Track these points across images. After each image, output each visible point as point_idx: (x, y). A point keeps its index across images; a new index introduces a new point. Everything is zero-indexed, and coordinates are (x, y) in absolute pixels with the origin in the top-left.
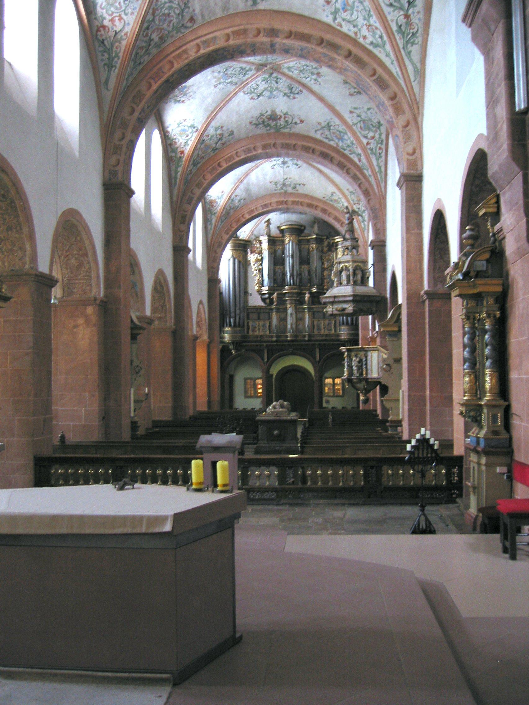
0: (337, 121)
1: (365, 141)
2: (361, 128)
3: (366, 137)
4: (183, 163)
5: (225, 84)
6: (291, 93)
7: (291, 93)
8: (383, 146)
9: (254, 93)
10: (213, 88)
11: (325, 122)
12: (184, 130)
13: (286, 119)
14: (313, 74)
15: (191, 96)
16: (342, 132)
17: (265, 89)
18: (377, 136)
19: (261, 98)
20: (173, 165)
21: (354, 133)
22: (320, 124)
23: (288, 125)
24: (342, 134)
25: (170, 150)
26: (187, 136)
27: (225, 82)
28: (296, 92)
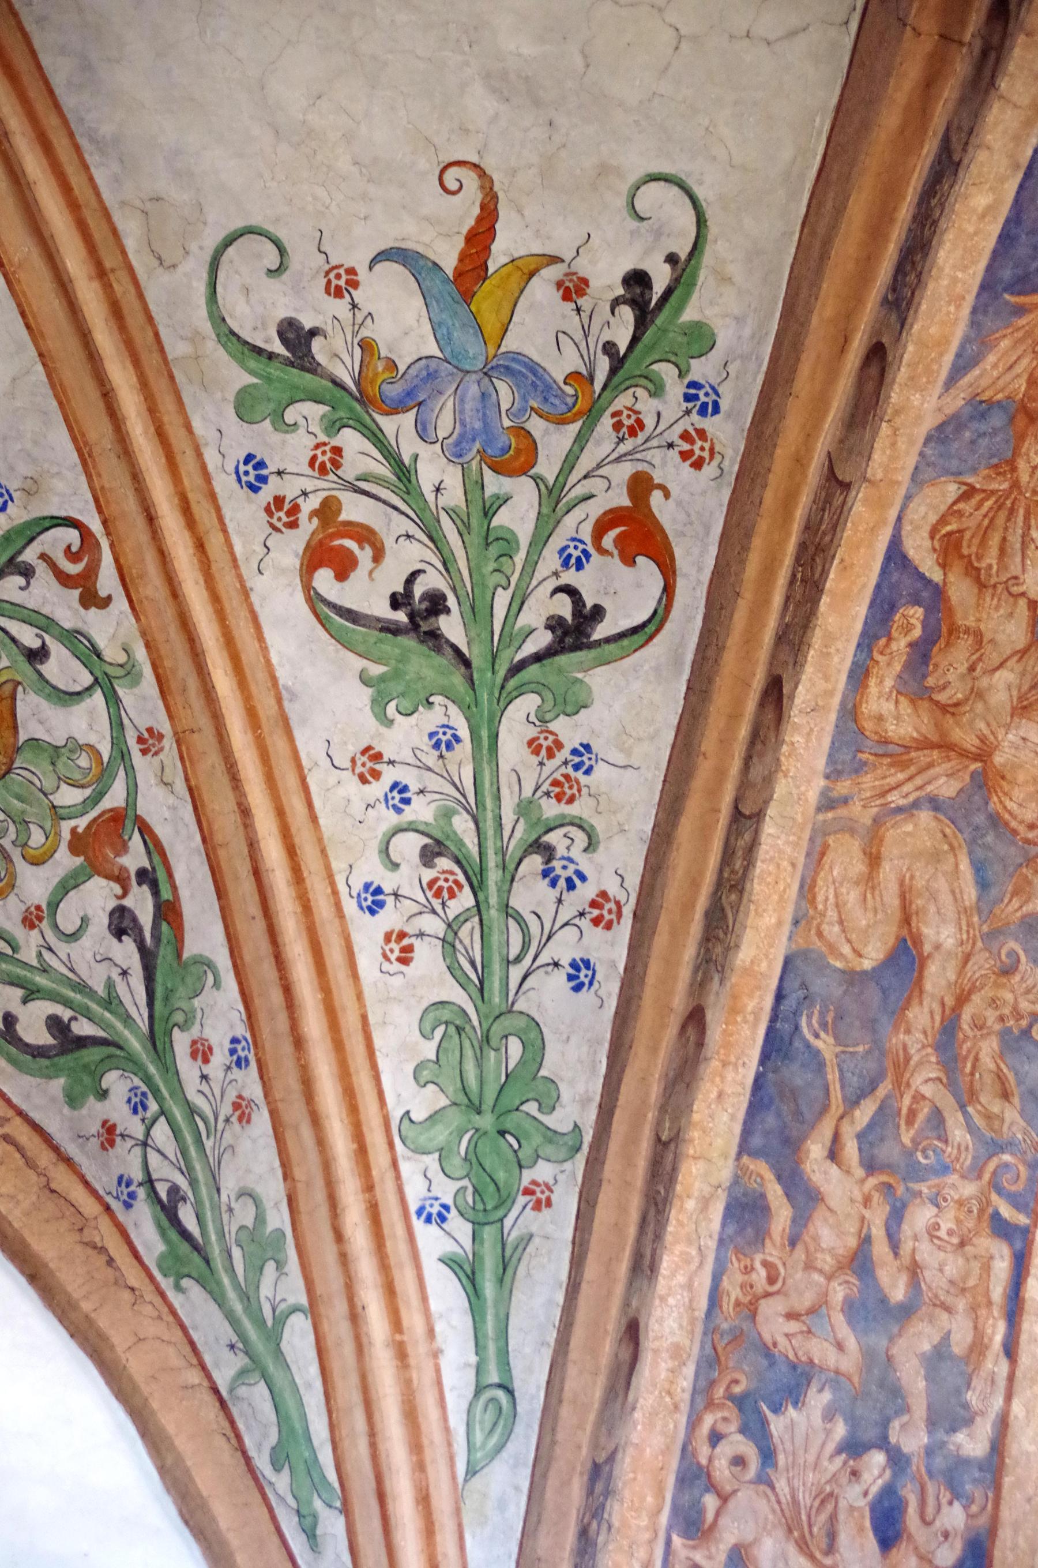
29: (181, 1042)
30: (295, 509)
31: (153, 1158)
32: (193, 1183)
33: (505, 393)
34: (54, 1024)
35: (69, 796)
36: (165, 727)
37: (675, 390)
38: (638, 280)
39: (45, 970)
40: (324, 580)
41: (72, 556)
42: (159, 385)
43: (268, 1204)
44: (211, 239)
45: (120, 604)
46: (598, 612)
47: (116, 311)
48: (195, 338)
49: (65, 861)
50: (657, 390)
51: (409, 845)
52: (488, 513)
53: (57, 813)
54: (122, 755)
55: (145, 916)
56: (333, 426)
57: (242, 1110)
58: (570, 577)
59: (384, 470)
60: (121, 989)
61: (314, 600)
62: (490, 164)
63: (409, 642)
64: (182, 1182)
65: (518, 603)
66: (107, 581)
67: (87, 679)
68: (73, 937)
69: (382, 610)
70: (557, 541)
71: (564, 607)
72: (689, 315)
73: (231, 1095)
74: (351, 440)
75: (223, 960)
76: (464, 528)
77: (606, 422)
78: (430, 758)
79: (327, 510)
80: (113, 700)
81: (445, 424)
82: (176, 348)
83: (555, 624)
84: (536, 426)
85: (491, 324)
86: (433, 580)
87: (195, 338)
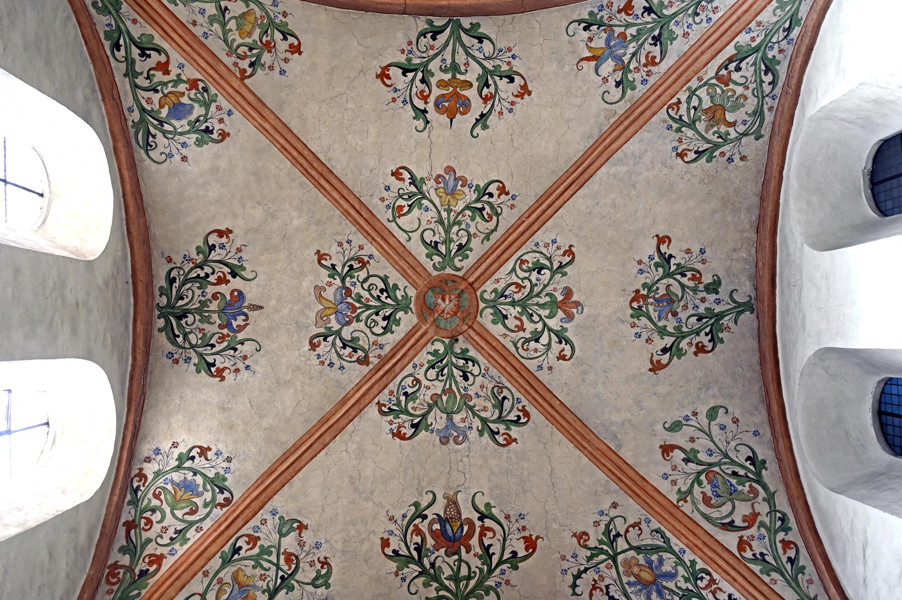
0: (633, 510)
1: (730, 540)
2: (706, 501)
3: (730, 526)
4: (144, 592)
5: (339, 344)
6: (499, 419)
7: (499, 419)
8: (794, 536)
9: (406, 412)
10: (308, 347)
11: (597, 524)
12: (188, 486)
13: (487, 542)
14: (554, 305)
15: (245, 358)
16: (656, 549)
17: (436, 399)
18: (763, 508)
19: (423, 434)
20: (109, 592)
21: (689, 527)
22: (581, 537)
23: (491, 571)
24: (654, 557)
25: (120, 540)
26: (193, 512)
27: (338, 333)
28: (512, 417)
29: (754, 45)
30: (647, 71)
31: (780, 39)
32: (780, 27)
33: (612, 43)
34: (766, 74)
35: (719, 91)
36: (696, 77)
37: (601, 14)
38: (585, 29)
39: (755, 81)
40: (657, 60)
41: (673, 109)
42: (636, 105)
43: (773, 8)
44: (608, 106)
45: (677, 96)
46: (644, 8)
47: (627, 118)
48: (626, 102)
49: (731, 86)
50: (602, 17)
51: (697, 19)
52: (634, 36)
53: (723, 91)
54: (706, 84)
55: (734, 64)
56: (631, 71)
57: (759, 24)
58: (640, 16)
59: (634, 59)
60: (751, 63)
61: (661, 60)
62: (576, 63)
63: (662, 39)
64: (781, 30)
65: (648, 23)
66: (674, 100)
67: (694, 97)
68: (746, 77)
69: (658, 47)
70: (635, 22)
71: (646, 14)
72: (587, 17)
73: (757, 28)
74: (632, 67)
75: (733, 44)
76: (639, 39)
77: (611, 23)
78: (681, 24)
79: (645, 65)
80: (696, 90)
81: (622, 51)
82: (629, 105)
83: (649, 14)
84: (616, 35)
85: (602, 51)
86: (650, 41)
87: (626, 102)
